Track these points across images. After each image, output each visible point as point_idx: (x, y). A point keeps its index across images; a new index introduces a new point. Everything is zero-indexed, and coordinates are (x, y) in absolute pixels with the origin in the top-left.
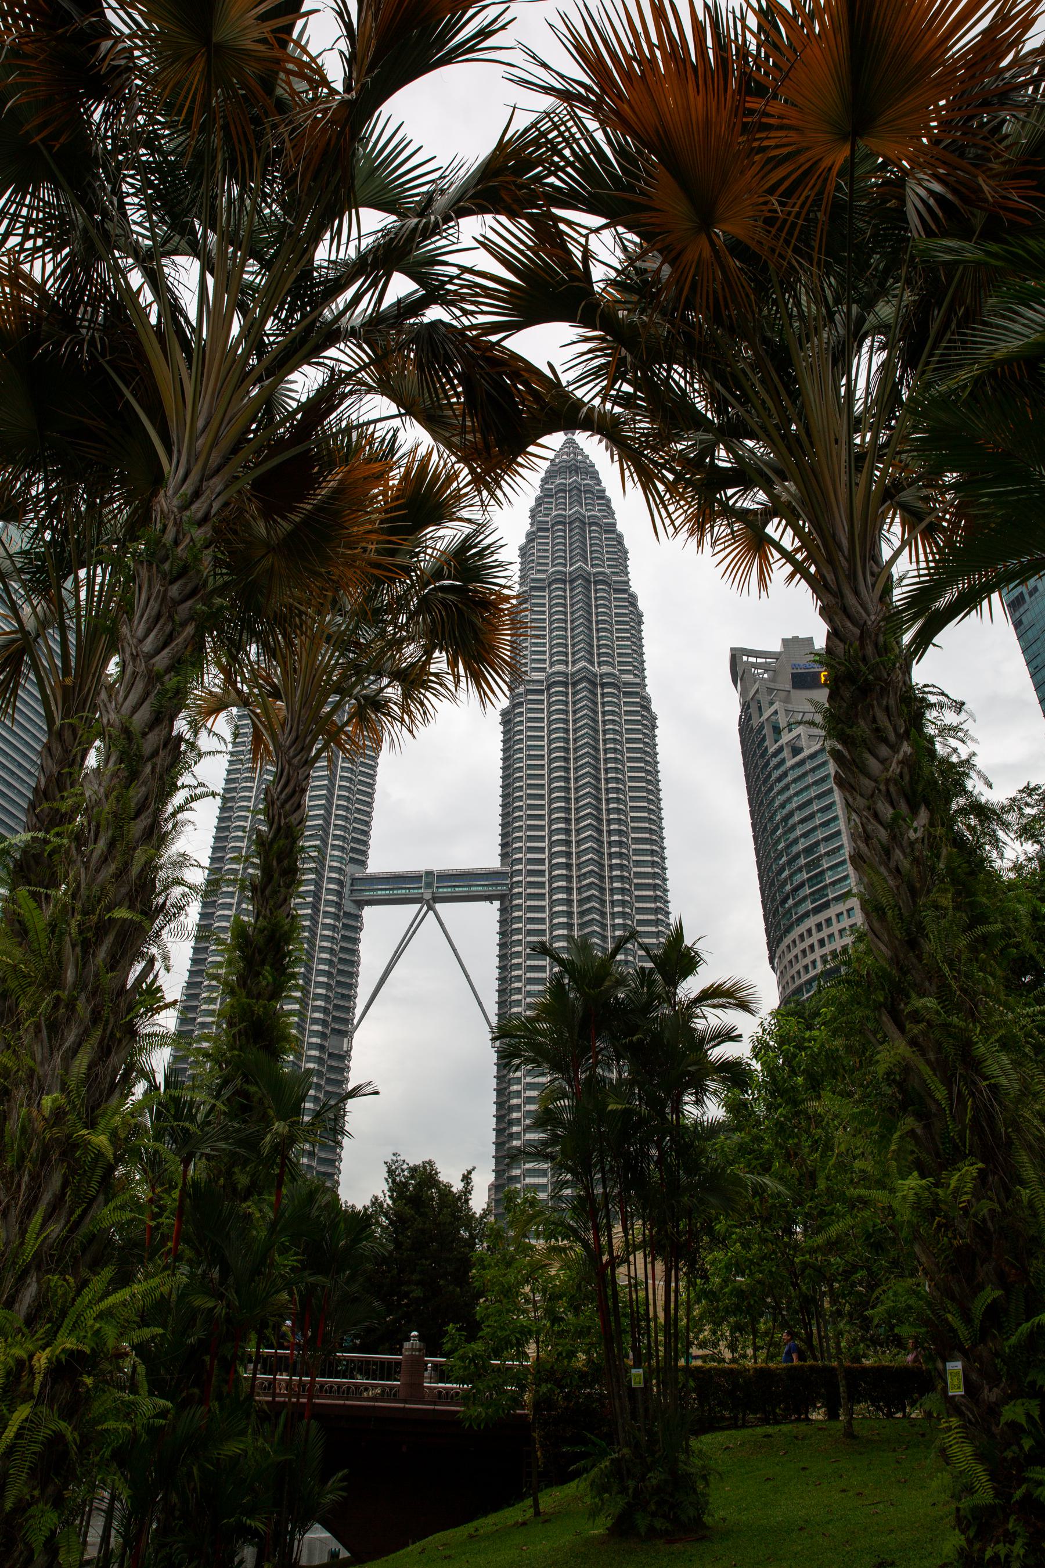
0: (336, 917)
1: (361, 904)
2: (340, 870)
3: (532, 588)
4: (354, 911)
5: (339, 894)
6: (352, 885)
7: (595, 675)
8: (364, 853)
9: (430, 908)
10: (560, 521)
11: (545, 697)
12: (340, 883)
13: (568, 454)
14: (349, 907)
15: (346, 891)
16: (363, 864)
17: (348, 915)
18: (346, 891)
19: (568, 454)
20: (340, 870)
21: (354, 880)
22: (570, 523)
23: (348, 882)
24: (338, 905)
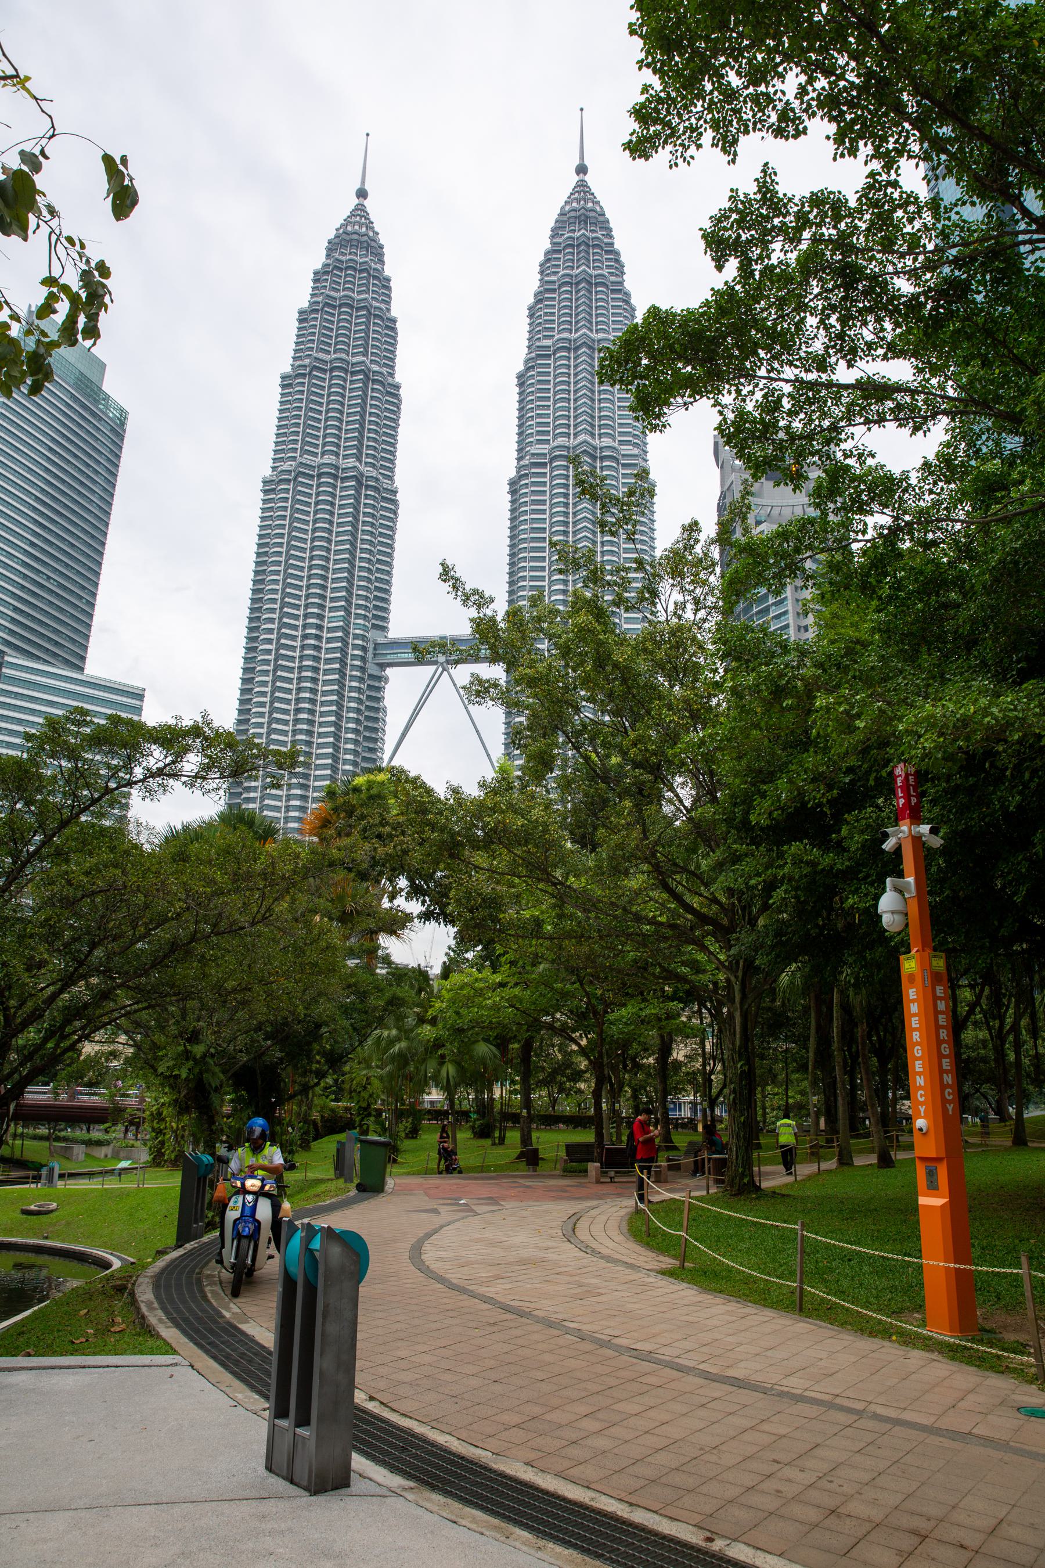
0: (361, 680)
1: (383, 666)
2: (363, 638)
3: (539, 356)
4: (377, 673)
5: (363, 659)
6: (375, 649)
7: (595, 448)
8: (385, 619)
9: (444, 670)
10: (569, 282)
11: (547, 470)
12: (364, 649)
13: (578, 201)
14: (373, 670)
15: (370, 655)
16: (384, 629)
17: (371, 676)
18: (370, 655)
19: (578, 201)
20: (363, 638)
21: (376, 646)
22: (577, 284)
23: (371, 646)
24: (362, 669)
